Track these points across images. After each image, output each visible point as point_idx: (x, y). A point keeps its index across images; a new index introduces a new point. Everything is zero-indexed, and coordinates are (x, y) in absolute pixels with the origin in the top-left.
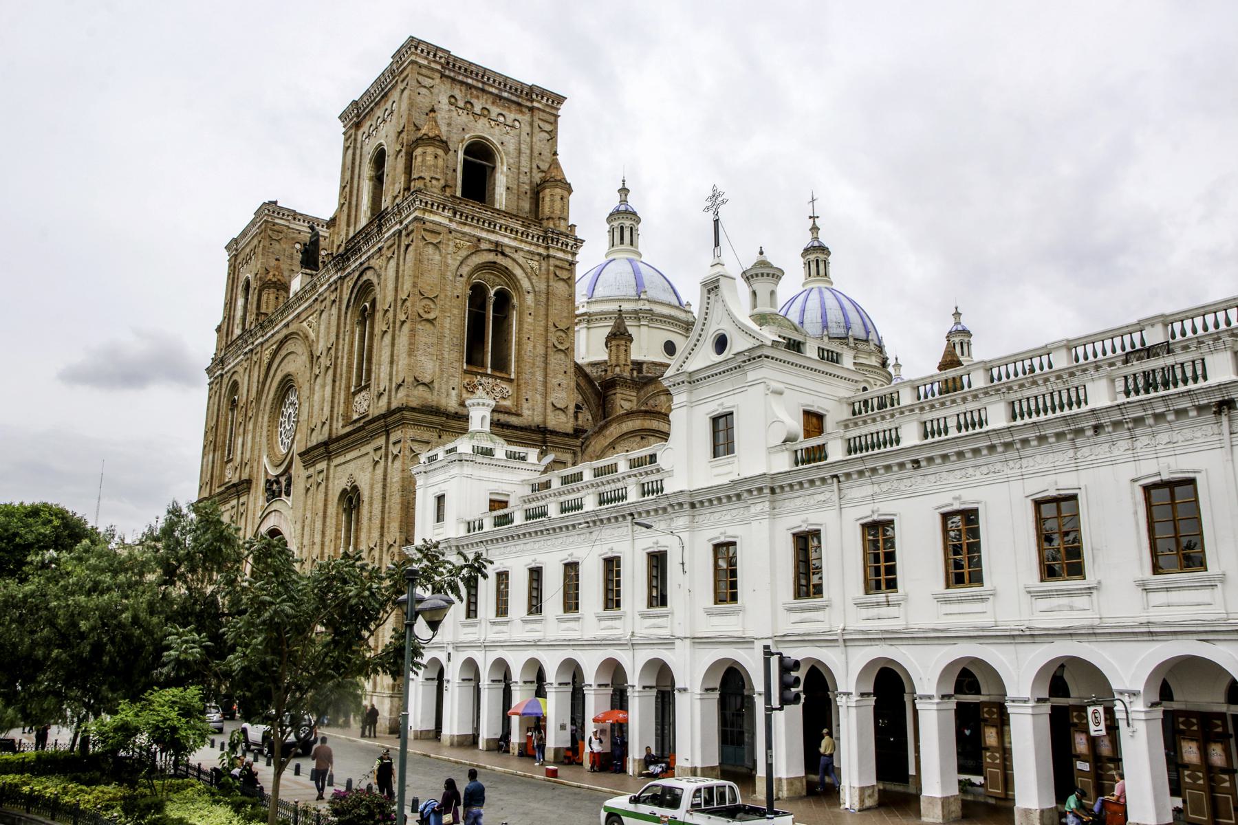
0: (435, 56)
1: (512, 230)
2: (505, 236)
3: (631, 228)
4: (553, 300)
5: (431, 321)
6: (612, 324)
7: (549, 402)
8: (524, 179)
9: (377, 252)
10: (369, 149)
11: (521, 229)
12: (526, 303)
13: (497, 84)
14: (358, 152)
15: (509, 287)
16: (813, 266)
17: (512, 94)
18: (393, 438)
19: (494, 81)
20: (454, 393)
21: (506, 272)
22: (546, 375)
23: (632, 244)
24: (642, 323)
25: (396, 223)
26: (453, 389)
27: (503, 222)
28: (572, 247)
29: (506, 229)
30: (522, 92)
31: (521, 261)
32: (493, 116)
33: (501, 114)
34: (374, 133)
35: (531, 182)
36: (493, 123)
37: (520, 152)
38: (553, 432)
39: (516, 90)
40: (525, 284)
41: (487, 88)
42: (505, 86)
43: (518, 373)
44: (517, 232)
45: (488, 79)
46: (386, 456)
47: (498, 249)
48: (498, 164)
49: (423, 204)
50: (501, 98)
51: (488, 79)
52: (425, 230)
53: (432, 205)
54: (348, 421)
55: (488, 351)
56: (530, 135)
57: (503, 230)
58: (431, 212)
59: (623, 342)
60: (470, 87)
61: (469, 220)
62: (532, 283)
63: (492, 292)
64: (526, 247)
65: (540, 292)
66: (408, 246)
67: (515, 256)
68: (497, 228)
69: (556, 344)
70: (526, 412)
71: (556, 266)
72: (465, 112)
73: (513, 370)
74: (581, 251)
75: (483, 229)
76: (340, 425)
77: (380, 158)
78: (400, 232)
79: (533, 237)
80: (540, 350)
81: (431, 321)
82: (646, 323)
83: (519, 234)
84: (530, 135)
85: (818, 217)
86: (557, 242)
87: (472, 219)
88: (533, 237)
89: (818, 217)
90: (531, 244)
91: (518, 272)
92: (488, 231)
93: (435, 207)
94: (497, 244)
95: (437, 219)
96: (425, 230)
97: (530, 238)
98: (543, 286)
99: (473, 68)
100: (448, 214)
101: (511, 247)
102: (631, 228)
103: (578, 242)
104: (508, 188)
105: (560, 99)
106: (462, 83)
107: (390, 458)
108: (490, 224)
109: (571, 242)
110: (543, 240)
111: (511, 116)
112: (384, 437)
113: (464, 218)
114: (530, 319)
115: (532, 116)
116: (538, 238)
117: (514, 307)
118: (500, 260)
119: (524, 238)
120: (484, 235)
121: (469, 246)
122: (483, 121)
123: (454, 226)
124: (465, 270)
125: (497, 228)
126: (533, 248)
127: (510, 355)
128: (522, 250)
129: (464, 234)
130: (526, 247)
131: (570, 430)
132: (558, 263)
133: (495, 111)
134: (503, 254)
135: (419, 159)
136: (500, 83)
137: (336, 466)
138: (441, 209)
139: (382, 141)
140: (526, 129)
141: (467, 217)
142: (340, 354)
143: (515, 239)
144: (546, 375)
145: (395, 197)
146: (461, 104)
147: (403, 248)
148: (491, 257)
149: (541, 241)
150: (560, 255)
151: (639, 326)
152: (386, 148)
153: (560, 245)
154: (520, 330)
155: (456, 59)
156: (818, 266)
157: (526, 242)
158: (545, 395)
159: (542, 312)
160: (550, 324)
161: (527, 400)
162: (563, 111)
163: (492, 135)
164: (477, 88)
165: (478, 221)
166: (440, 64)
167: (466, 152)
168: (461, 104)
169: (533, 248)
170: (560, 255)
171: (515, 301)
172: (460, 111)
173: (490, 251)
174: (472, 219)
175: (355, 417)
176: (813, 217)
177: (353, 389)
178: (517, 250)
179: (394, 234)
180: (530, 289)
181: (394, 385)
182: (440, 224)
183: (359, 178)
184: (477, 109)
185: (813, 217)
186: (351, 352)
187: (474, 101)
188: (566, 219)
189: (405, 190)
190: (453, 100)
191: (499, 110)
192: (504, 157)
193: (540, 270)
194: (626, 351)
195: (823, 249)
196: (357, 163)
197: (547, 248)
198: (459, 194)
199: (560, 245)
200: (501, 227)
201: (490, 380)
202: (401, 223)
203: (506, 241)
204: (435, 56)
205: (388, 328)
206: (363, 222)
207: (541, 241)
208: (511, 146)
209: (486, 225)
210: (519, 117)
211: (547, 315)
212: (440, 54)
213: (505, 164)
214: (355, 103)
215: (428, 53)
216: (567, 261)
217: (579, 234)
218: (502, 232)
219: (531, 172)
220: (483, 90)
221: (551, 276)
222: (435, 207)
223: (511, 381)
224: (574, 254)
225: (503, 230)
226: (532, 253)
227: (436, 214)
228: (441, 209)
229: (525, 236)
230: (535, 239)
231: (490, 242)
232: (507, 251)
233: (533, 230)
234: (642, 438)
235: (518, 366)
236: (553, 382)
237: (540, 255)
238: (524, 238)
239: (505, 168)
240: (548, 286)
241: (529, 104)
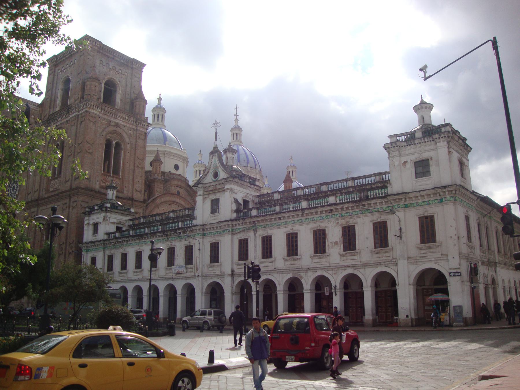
0: (95, 43)
1: (123, 118)
3: (162, 115)
5: (90, 153)
6: (155, 155)
7: (134, 188)
9: (65, 122)
10: (62, 77)
11: (127, 118)
14: (56, 77)
15: (121, 141)
16: (235, 136)
18: (72, 200)
20: (98, 183)
21: (120, 135)
23: (162, 122)
24: (166, 156)
25: (77, 111)
26: (98, 181)
28: (146, 126)
29: (121, 117)
31: (126, 130)
32: (117, 70)
33: (120, 69)
34: (65, 70)
35: (130, 98)
36: (117, 73)
37: (126, 85)
38: (135, 201)
40: (127, 140)
43: (123, 176)
44: (125, 119)
45: (116, 54)
46: (69, 207)
47: (117, 125)
48: (118, 90)
49: (90, 105)
52: (90, 116)
53: (93, 106)
54: (47, 191)
57: (120, 118)
58: (92, 109)
59: (159, 164)
61: (107, 113)
62: (130, 140)
63: (114, 143)
65: (133, 144)
66: (82, 122)
67: (124, 129)
68: (118, 117)
69: (138, 165)
70: (125, 192)
71: (139, 134)
72: (106, 67)
73: (121, 175)
76: (44, 193)
77: (67, 81)
78: (78, 115)
80: (132, 167)
81: (90, 153)
82: (167, 156)
85: (238, 115)
86: (141, 124)
87: (108, 112)
88: (131, 121)
89: (238, 115)
91: (125, 135)
92: (114, 118)
93: (94, 107)
95: (95, 112)
96: (90, 116)
97: (130, 122)
100: (99, 110)
101: (122, 125)
102: (162, 115)
104: (121, 100)
107: (71, 208)
108: (115, 115)
109: (146, 125)
110: (135, 123)
112: (68, 199)
113: (105, 112)
114: (128, 155)
116: (133, 122)
118: (118, 130)
119: (128, 122)
120: (112, 119)
121: (106, 124)
123: (101, 115)
124: (104, 133)
125: (118, 117)
126: (131, 126)
127: (119, 168)
128: (127, 126)
129: (105, 119)
131: (142, 201)
133: (118, 68)
135: (88, 87)
137: (41, 210)
138: (96, 108)
139: (69, 75)
143: (124, 122)
145: (76, 100)
146: (105, 64)
147: (79, 122)
148: (115, 128)
149: (134, 123)
150: (142, 129)
151: (165, 157)
152: (71, 78)
153: (142, 125)
156: (237, 136)
157: (128, 123)
158: (133, 185)
160: (136, 157)
161: (126, 187)
162: (145, 70)
165: (111, 113)
166: (97, 46)
167: (105, 84)
168: (105, 64)
169: (131, 126)
170: (142, 129)
171: (123, 147)
172: (104, 67)
173: (114, 126)
174: (108, 112)
175: (51, 190)
176: (236, 115)
179: (75, 116)
180: (129, 142)
181: (73, 178)
182: (96, 114)
183: (56, 88)
185: (236, 115)
187: (110, 63)
188: (144, 115)
189: (81, 98)
190: (101, 62)
191: (119, 68)
192: (120, 87)
193: (133, 135)
194: (160, 168)
195: (240, 129)
196: (55, 82)
197: (137, 126)
198: (102, 101)
199: (142, 125)
200: (119, 117)
202: (79, 112)
203: (121, 122)
204: (95, 43)
205: (71, 154)
206: (58, 108)
207: (134, 123)
209: (114, 115)
210: (127, 70)
213: (120, 90)
214: (55, 56)
216: (144, 132)
219: (130, 94)
221: (138, 138)
222: (94, 107)
223: (119, 179)
225: (120, 118)
226: (131, 128)
227: (94, 110)
229: (128, 121)
230: (132, 122)
231: (115, 123)
233: (132, 119)
234: (169, 204)
235: (123, 173)
237: (133, 129)
238: (128, 122)
239: (120, 92)
240: (136, 142)
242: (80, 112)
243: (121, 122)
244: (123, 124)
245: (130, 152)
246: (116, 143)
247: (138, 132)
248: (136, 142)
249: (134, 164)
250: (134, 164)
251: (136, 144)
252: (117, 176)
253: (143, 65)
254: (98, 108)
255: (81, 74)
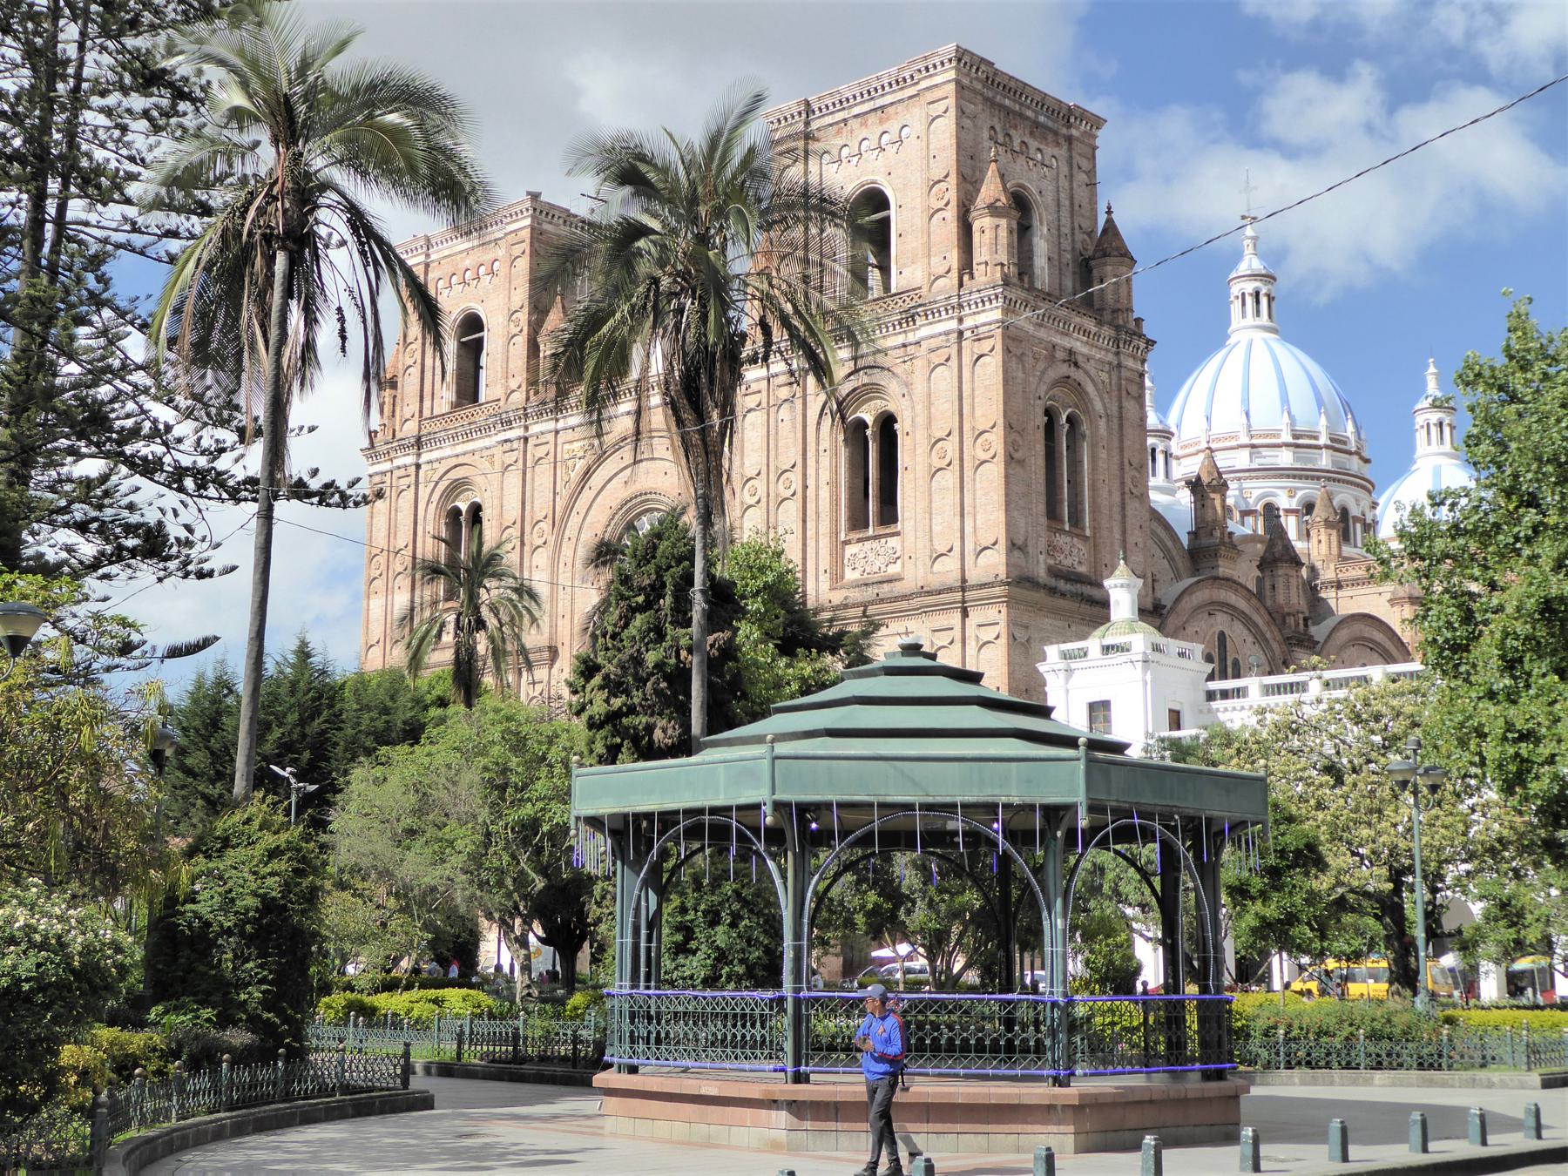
4: (1126, 425)
8: (1066, 245)
11: (1094, 329)
12: (1098, 429)
20: (1042, 558)
21: (1078, 388)
22: (1124, 532)
31: (1093, 372)
32: (1032, 151)
35: (1073, 249)
40: (1098, 406)
43: (1095, 529)
47: (1072, 359)
48: (1036, 222)
50: (1037, 125)
54: (837, 578)
55: (1062, 501)
56: (1071, 177)
60: (1008, 112)
63: (1064, 417)
67: (1088, 367)
74: (1150, 356)
80: (1116, 498)
84: (1071, 177)
91: (1090, 388)
94: (1071, 352)
98: (1115, 408)
99: (1012, 84)
103: (1150, 343)
105: (1098, 122)
106: (1001, 107)
111: (1049, 150)
114: (1103, 454)
115: (1070, 149)
117: (1084, 437)
120: (1057, 339)
122: (1021, 160)
127: (1082, 502)
132: (1128, 374)
133: (1033, 144)
134: (1076, 364)
140: (1064, 170)
142: (811, 482)
144: (1124, 532)
154: (1094, 469)
155: (997, 72)
156: (1258, 302)
159: (1116, 443)
162: (1103, 138)
163: (1030, 181)
164: (1014, 112)
175: (850, 575)
177: (842, 537)
179: (947, 333)
184: (1016, 145)
186: (834, 484)
187: (1012, 132)
188: (1129, 310)
197: (1117, 354)
201: (1068, 539)
208: (1049, 197)
210: (1056, 152)
211: (1121, 450)
212: (983, 67)
217: (1147, 330)
220: (1021, 115)
224: (1143, 361)
232: (1080, 359)
235: (1094, 520)
236: (1131, 540)
239: (1045, 230)
240: (1121, 408)
241: (1064, 131)
242: (968, 322)
243: (1079, 345)
244: (1085, 350)
246: (1069, 419)
247: (1124, 373)
248: (1121, 408)
249: (1123, 483)
250: (1123, 483)
251: (1121, 418)
252: (1078, 531)
253: (1098, 122)
255: (943, 185)
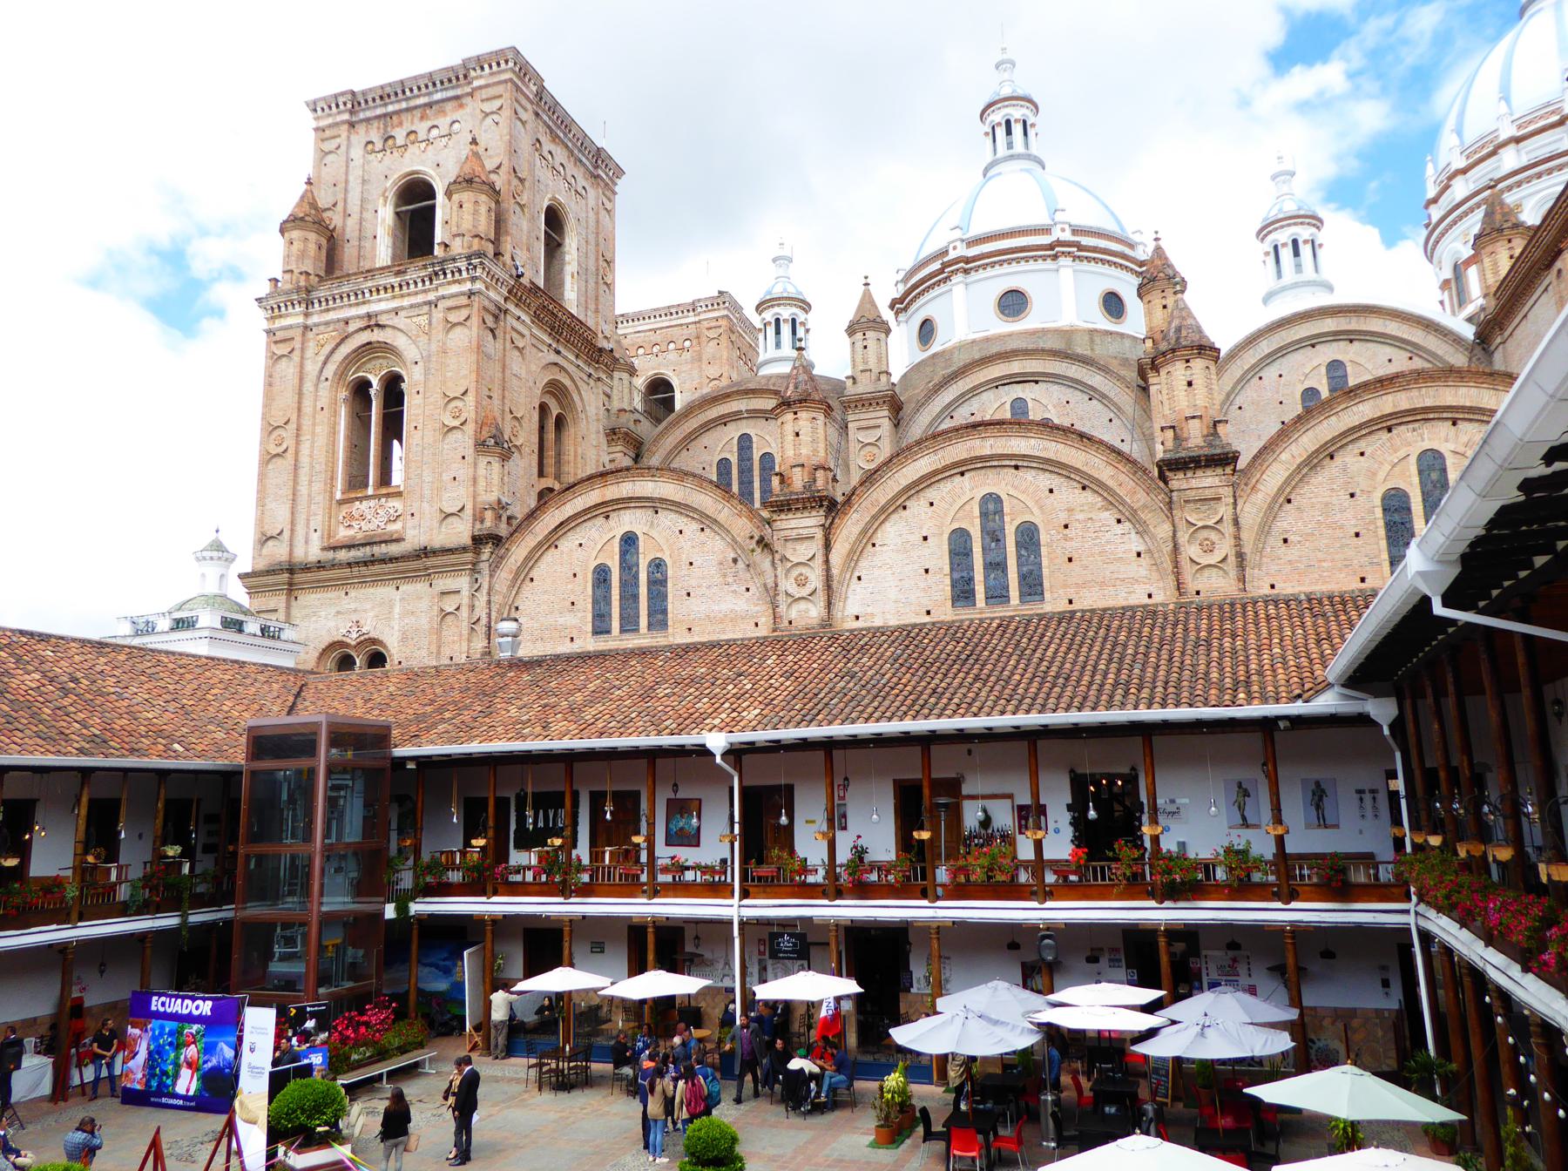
2: (380, 300)
11: (395, 280)
13: (424, 90)
17: (446, 89)
19: (419, 88)
27: (370, 284)
29: (386, 289)
30: (458, 78)
39: (450, 81)
41: (413, 103)
42: (434, 84)
45: (411, 90)
51: (411, 90)
64: (406, 302)
68: (367, 295)
75: (350, 305)
79: (416, 283)
83: (397, 289)
90: (416, 293)
92: (357, 304)
94: (369, 316)
99: (388, 90)
118: (377, 336)
128: (402, 308)
130: (406, 302)
136: (427, 86)
138: (290, 308)
141: (327, 300)
143: (394, 297)
165: (342, 298)
178: (396, 312)
204: (337, 106)
209: (352, 298)
215: (330, 107)
218: (375, 296)
228: (290, 308)
230: (420, 284)
231: (360, 317)
232: (383, 320)
245: (421, 390)
254: (293, 305)
